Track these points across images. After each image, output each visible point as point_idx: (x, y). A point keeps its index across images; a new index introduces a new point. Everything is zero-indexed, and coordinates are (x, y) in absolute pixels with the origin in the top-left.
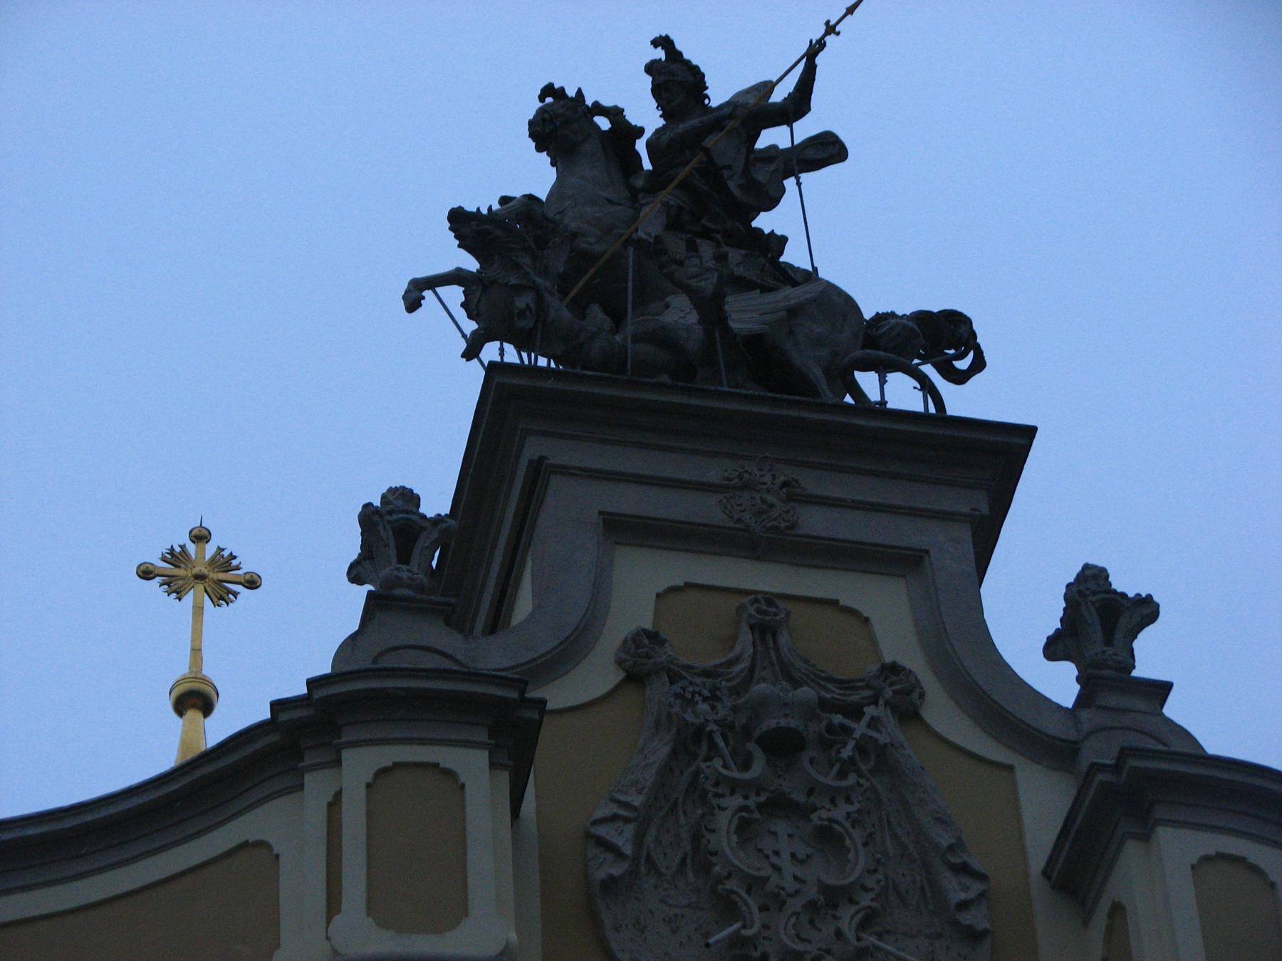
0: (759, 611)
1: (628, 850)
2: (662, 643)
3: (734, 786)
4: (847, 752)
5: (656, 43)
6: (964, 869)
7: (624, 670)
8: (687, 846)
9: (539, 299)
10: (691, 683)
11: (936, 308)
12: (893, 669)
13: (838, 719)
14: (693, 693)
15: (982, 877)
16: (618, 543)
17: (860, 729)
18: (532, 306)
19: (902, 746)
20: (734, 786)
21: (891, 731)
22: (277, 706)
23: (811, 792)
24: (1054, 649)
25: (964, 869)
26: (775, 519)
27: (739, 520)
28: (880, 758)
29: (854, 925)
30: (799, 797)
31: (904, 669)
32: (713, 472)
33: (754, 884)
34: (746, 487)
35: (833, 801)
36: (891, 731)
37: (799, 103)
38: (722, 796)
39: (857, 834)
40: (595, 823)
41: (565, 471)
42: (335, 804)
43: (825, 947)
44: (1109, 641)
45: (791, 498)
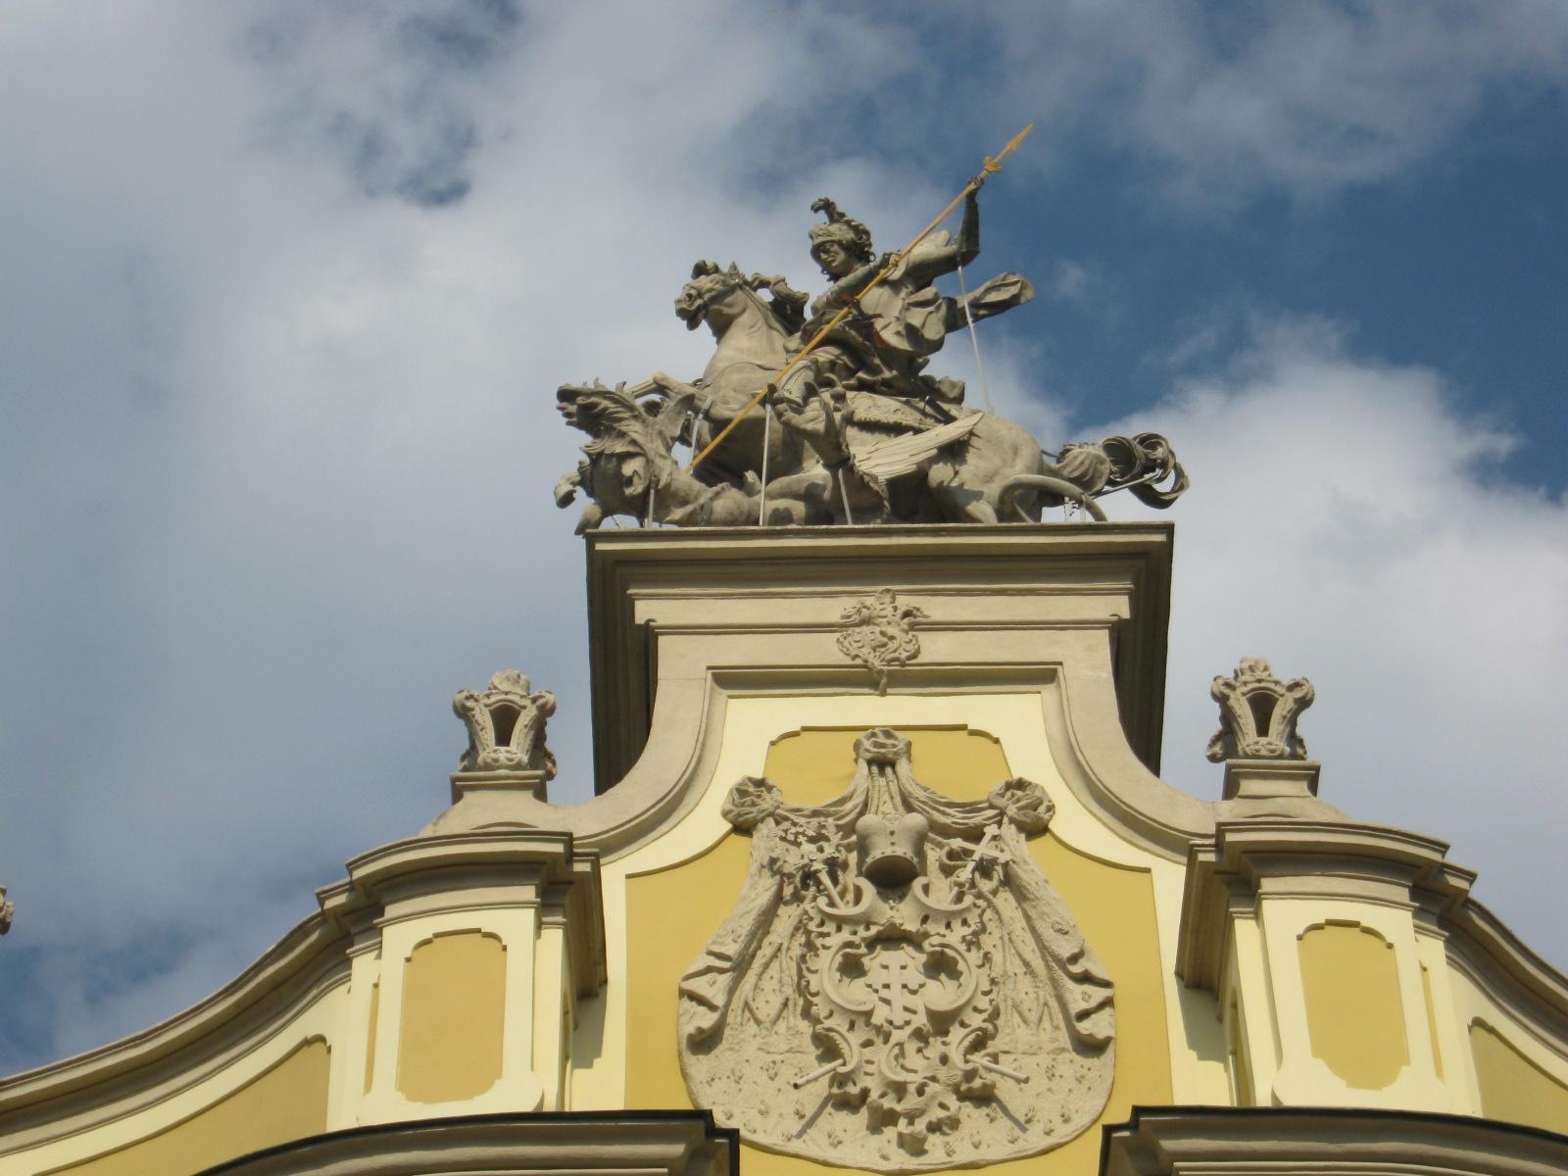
0: (877, 745)
1: (719, 1000)
2: (770, 789)
3: (840, 922)
5: (815, 209)
6: (1086, 978)
7: (731, 822)
8: (789, 991)
10: (795, 824)
12: (1021, 785)
13: (957, 843)
14: (797, 834)
15: (1107, 984)
16: (730, 697)
17: (982, 850)
18: (641, 472)
19: (1025, 862)
20: (840, 922)
21: (1013, 846)
23: (925, 920)
25: (1086, 978)
26: (895, 651)
27: (857, 656)
29: (962, 1049)
30: (912, 926)
31: (1030, 784)
32: (832, 607)
34: (866, 622)
35: (948, 926)
36: (1013, 846)
38: (828, 935)
40: (688, 977)
43: (929, 1075)
44: (1263, 729)
45: (912, 627)
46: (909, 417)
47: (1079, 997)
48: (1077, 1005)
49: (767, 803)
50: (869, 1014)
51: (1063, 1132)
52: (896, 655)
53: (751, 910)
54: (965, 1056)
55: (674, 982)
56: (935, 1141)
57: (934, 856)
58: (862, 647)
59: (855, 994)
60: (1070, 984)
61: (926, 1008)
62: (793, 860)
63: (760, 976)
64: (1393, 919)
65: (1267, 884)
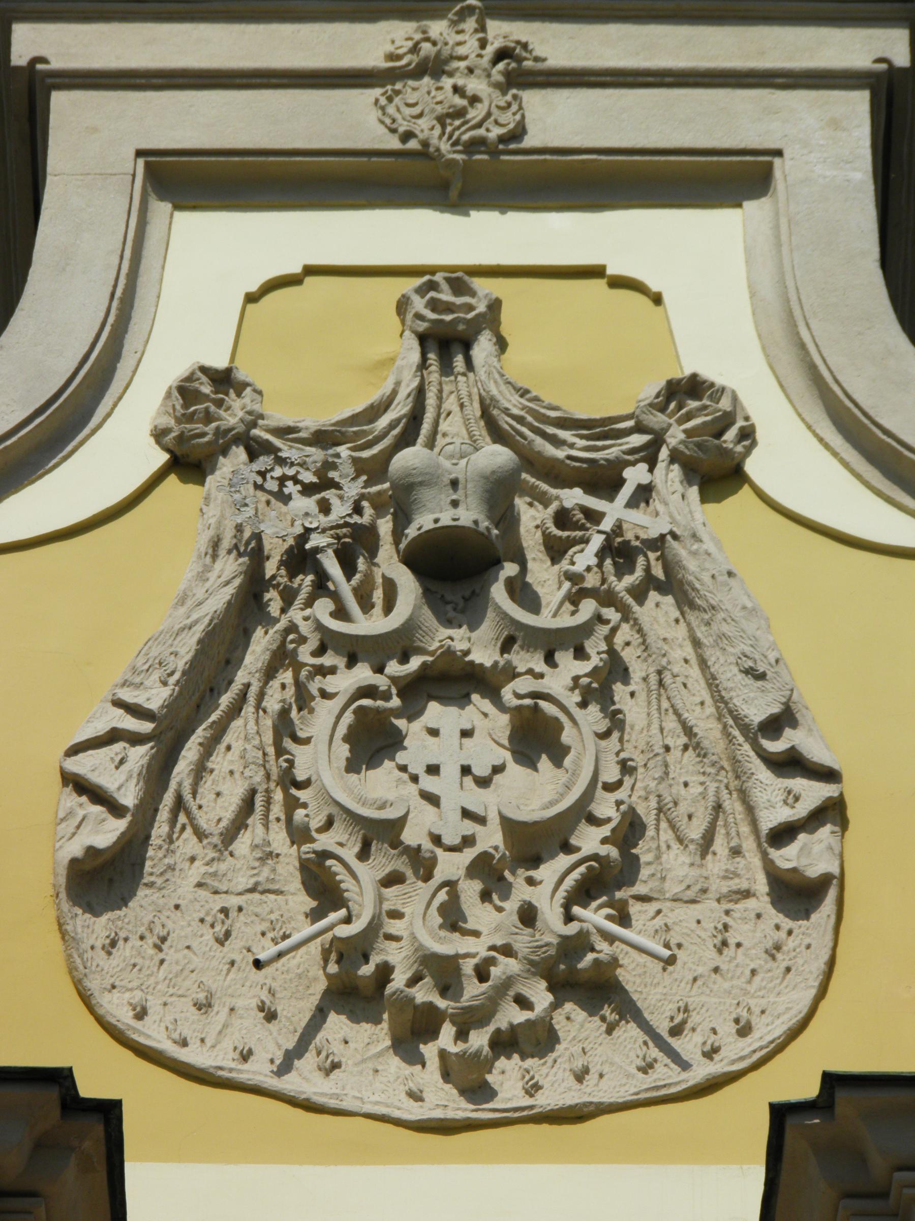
0: (434, 305)
1: (129, 798)
2: (241, 387)
3: (354, 651)
6: (791, 764)
7: (168, 450)
10: (281, 462)
13: (574, 497)
14: (282, 480)
15: (829, 775)
17: (614, 511)
19: (695, 537)
20: (354, 651)
23: (507, 646)
25: (791, 764)
26: (479, 125)
27: (407, 136)
28: (650, 568)
29: (561, 894)
30: (484, 655)
31: (712, 385)
33: (380, 833)
35: (550, 660)
38: (333, 670)
40: (75, 750)
43: (499, 942)
48: (774, 815)
49: (233, 415)
50: (400, 823)
52: (481, 132)
53: (196, 622)
54: (567, 907)
55: (52, 757)
57: (532, 519)
58: (420, 115)
59: (380, 789)
60: (763, 774)
61: (500, 813)
62: (278, 529)
63: (208, 749)
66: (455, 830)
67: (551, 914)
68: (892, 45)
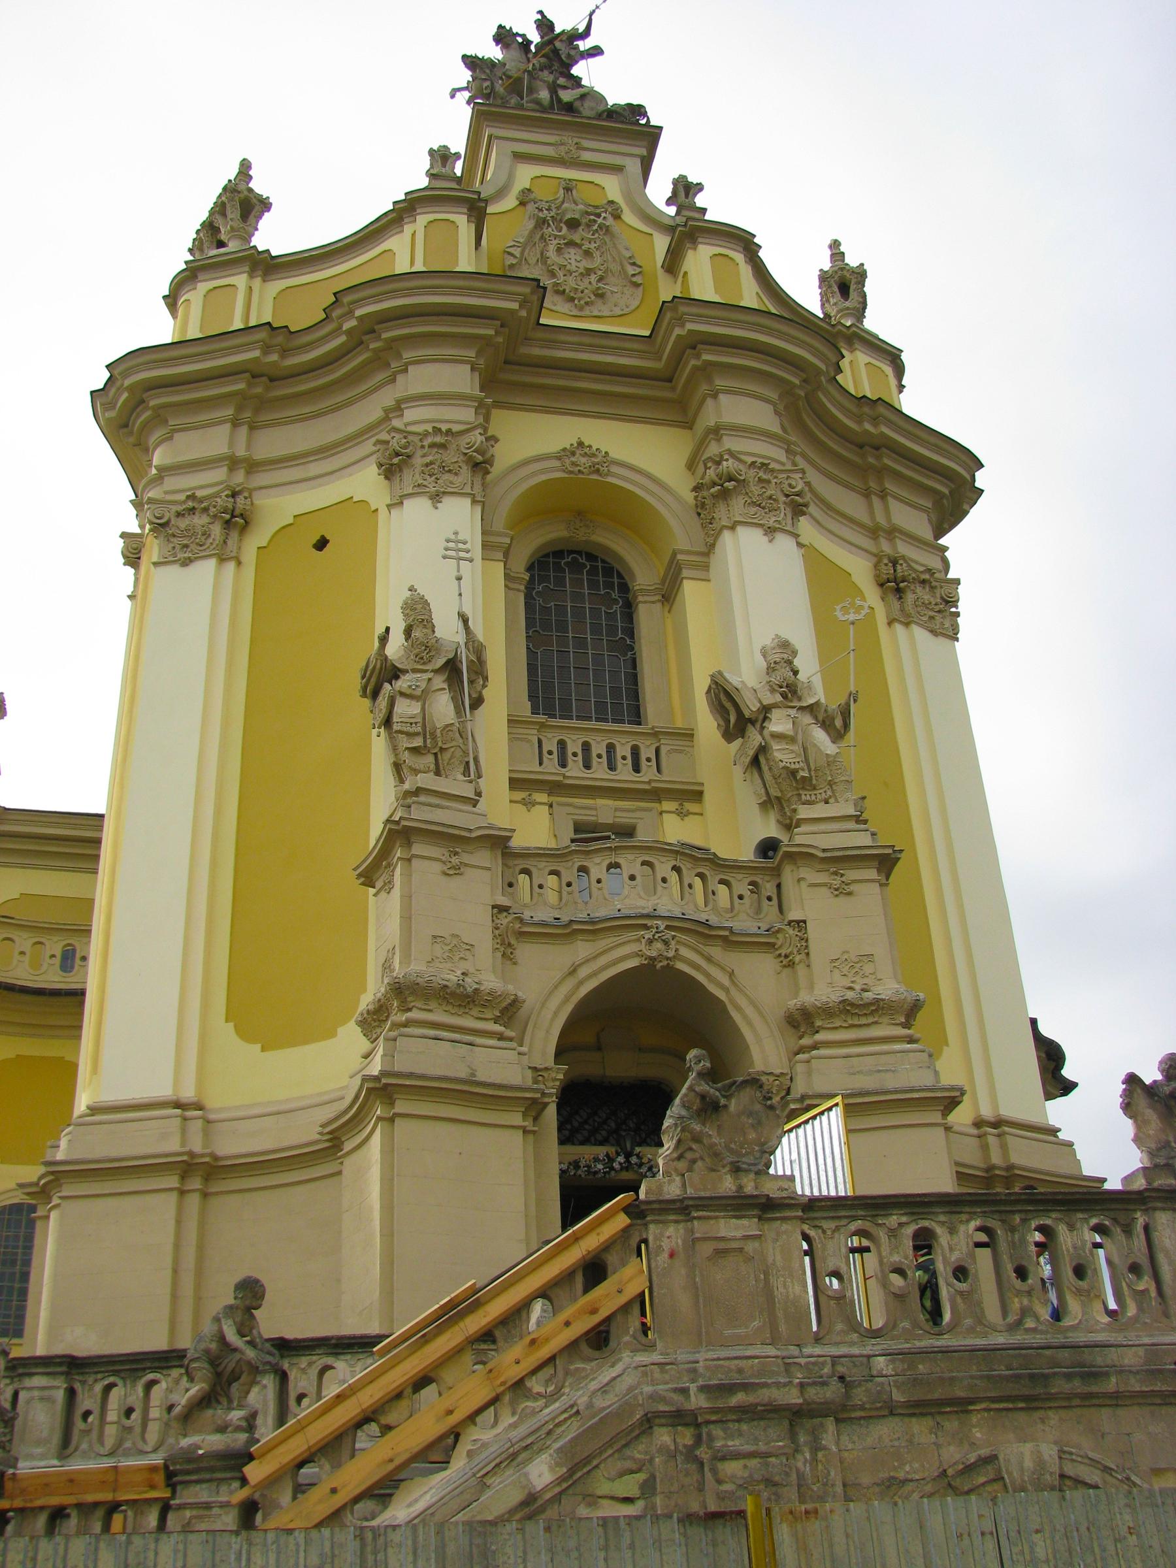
3: (556, 237)
4: (595, 228)
6: (634, 264)
8: (539, 256)
9: (492, 84)
11: (635, 103)
12: (612, 202)
17: (600, 221)
20: (556, 237)
21: (610, 221)
22: (395, 203)
24: (669, 202)
25: (634, 264)
28: (607, 230)
30: (578, 241)
34: (562, 144)
36: (610, 221)
37: (587, 33)
39: (598, 253)
41: (498, 138)
42: (414, 235)
44: (687, 196)
46: (569, 85)
47: (631, 270)
49: (532, 196)
51: (626, 311)
56: (588, 308)
57: (584, 221)
64: (739, 257)
65: (700, 240)
66: (574, 269)
67: (594, 283)
68: (644, 152)
